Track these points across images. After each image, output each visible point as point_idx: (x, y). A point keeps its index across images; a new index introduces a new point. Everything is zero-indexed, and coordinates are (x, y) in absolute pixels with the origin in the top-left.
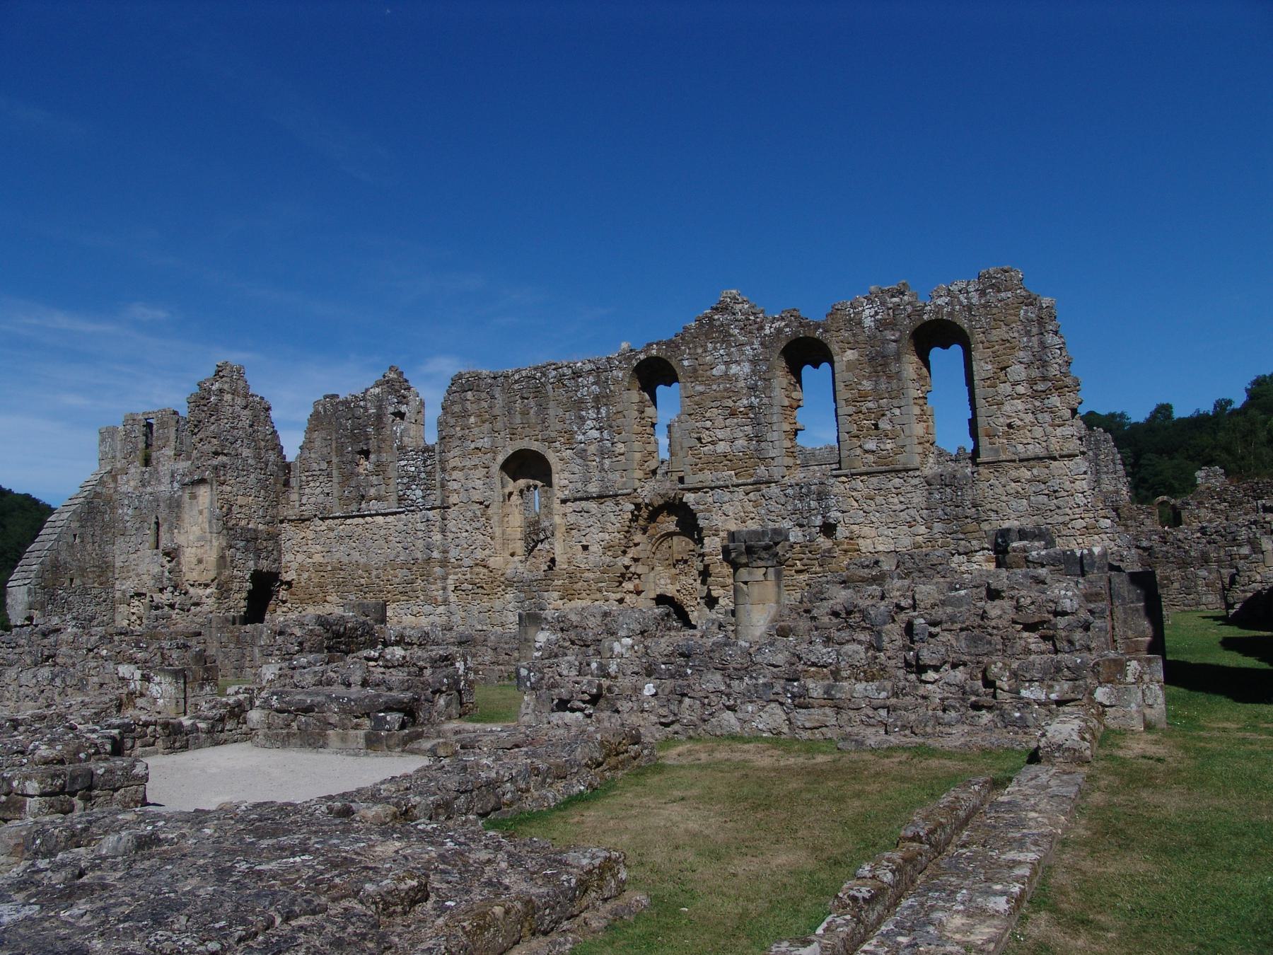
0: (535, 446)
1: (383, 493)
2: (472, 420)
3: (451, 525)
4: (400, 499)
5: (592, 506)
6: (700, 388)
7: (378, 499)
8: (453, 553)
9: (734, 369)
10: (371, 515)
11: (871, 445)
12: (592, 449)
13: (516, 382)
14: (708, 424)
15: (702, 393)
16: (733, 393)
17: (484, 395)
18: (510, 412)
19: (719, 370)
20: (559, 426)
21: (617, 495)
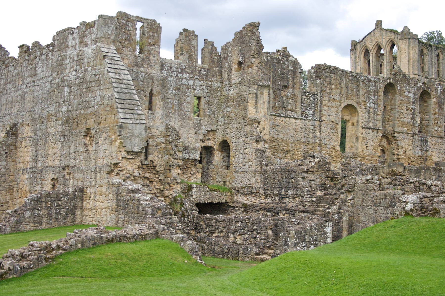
0: (355, 104)
1: (294, 108)
2: (333, 86)
3: (323, 129)
4: (302, 114)
5: (370, 131)
6: (402, 98)
7: (292, 111)
8: (323, 142)
9: (410, 95)
10: (289, 118)
11: (436, 129)
12: (372, 110)
13: (350, 76)
14: (402, 111)
15: (402, 100)
16: (408, 103)
17: (338, 78)
18: (347, 87)
19: (406, 94)
20: (363, 99)
21: (379, 129)
